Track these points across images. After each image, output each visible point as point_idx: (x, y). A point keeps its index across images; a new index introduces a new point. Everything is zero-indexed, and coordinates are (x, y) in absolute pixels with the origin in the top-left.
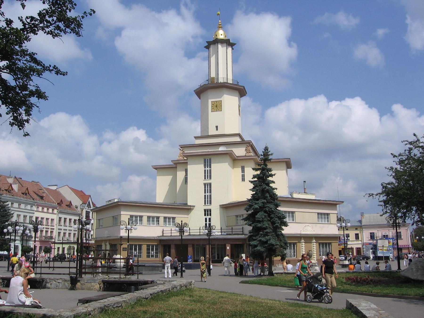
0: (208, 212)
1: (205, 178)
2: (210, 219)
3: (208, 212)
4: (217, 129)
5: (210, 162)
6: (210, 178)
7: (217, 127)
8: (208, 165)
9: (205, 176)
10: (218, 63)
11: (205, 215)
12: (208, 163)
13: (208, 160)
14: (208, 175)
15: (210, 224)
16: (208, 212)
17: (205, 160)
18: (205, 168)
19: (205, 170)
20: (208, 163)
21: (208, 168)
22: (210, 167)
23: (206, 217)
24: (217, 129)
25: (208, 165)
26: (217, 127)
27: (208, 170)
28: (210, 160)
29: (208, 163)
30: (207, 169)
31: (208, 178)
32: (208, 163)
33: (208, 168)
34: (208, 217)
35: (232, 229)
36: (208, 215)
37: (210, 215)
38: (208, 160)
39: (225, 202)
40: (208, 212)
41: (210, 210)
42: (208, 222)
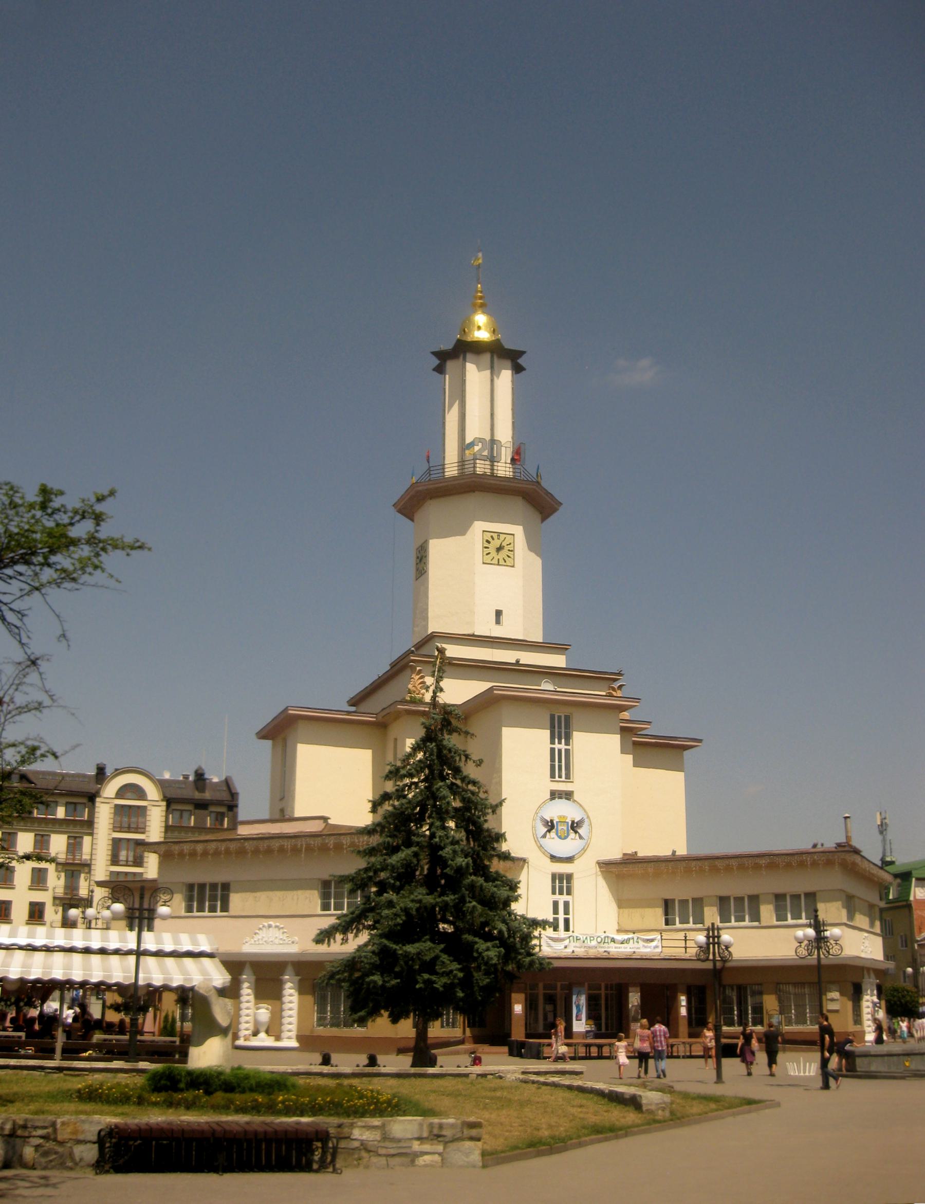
0: (561, 881)
1: (552, 775)
2: (566, 904)
3: (561, 881)
4: (498, 622)
5: (568, 726)
6: (568, 776)
7: (499, 613)
8: (560, 733)
9: (552, 767)
10: (492, 415)
11: (554, 893)
12: (561, 729)
13: (559, 717)
14: (561, 765)
15: (567, 921)
16: (562, 883)
17: (552, 717)
18: (552, 742)
19: (552, 750)
20: (561, 729)
21: (560, 743)
22: (567, 744)
23: (557, 897)
24: (498, 622)
25: (560, 733)
26: (499, 613)
27: (560, 751)
28: (568, 719)
29: (560, 727)
30: (557, 746)
31: (560, 777)
32: (560, 727)
33: (560, 743)
34: (562, 899)
35: (686, 940)
36: (561, 893)
37: (569, 893)
38: (559, 717)
39: (616, 855)
40: (562, 883)
41: (569, 877)
42: (561, 916)
